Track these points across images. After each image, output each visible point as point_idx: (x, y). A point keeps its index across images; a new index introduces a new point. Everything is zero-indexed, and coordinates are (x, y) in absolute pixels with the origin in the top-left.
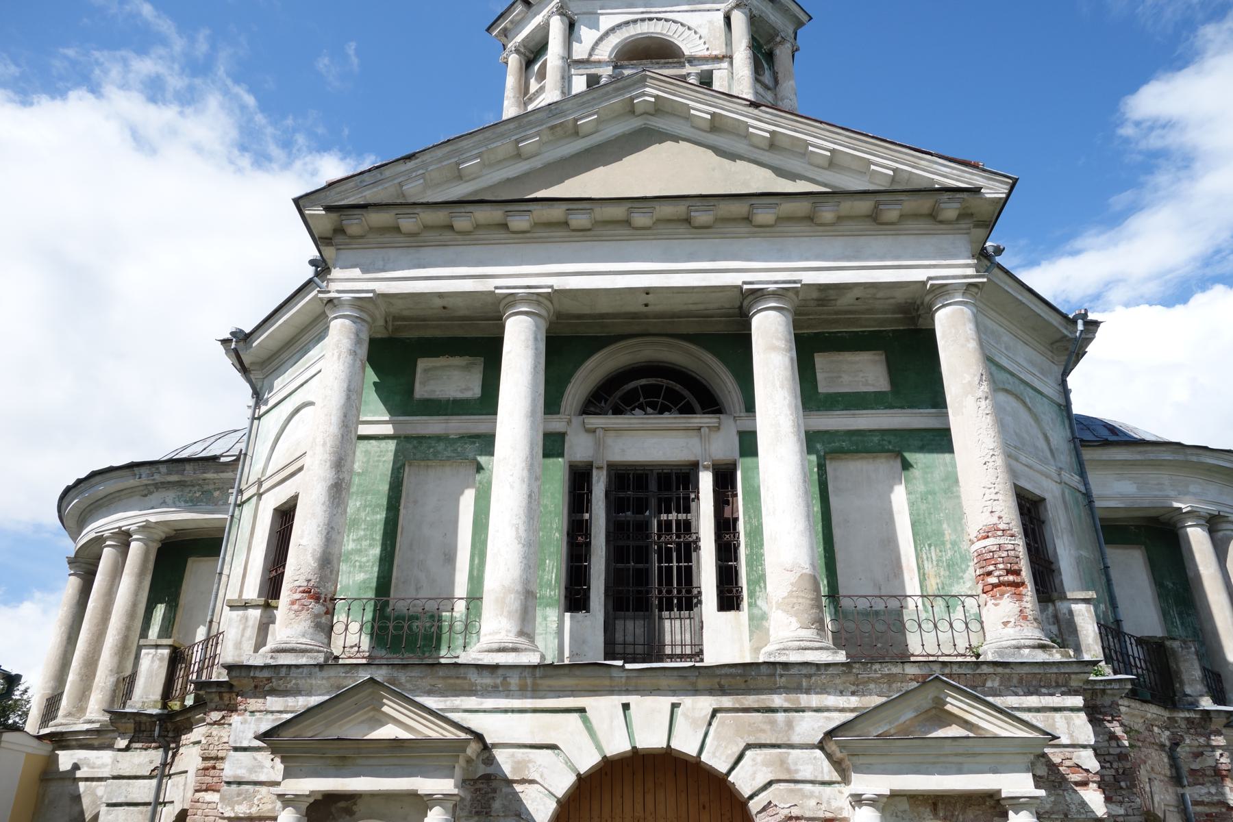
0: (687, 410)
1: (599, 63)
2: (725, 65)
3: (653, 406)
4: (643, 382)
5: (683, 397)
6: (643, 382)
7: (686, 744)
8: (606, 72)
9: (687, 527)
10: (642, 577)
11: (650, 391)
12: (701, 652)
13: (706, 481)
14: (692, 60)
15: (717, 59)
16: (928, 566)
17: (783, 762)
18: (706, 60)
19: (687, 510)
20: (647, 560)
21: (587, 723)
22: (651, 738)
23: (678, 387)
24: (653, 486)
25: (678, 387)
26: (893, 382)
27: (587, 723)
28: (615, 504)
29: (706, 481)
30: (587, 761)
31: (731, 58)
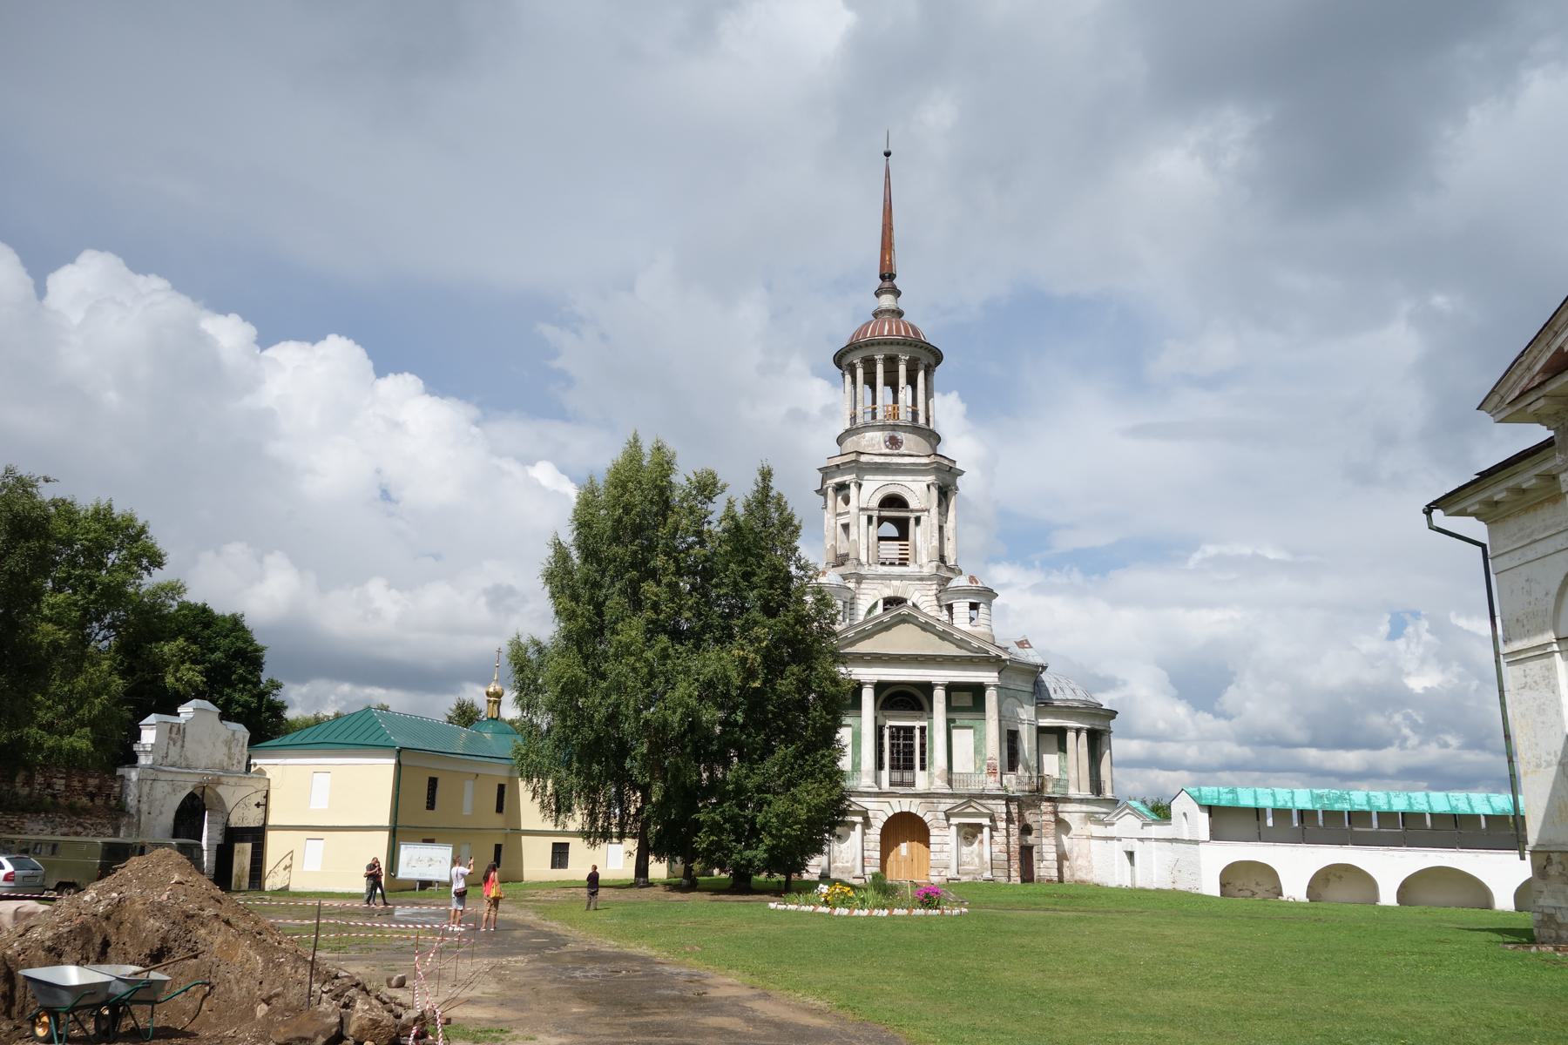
0: (913, 709)
1: (872, 510)
2: (926, 513)
4: (898, 698)
5: (910, 703)
6: (898, 698)
9: (912, 746)
10: (898, 759)
11: (902, 701)
12: (914, 782)
13: (917, 733)
14: (912, 511)
15: (923, 511)
16: (977, 762)
17: (935, 815)
18: (917, 511)
20: (904, 759)
22: (905, 809)
24: (902, 732)
26: (974, 704)
28: (892, 737)
29: (917, 733)
30: (891, 814)
31: (929, 511)
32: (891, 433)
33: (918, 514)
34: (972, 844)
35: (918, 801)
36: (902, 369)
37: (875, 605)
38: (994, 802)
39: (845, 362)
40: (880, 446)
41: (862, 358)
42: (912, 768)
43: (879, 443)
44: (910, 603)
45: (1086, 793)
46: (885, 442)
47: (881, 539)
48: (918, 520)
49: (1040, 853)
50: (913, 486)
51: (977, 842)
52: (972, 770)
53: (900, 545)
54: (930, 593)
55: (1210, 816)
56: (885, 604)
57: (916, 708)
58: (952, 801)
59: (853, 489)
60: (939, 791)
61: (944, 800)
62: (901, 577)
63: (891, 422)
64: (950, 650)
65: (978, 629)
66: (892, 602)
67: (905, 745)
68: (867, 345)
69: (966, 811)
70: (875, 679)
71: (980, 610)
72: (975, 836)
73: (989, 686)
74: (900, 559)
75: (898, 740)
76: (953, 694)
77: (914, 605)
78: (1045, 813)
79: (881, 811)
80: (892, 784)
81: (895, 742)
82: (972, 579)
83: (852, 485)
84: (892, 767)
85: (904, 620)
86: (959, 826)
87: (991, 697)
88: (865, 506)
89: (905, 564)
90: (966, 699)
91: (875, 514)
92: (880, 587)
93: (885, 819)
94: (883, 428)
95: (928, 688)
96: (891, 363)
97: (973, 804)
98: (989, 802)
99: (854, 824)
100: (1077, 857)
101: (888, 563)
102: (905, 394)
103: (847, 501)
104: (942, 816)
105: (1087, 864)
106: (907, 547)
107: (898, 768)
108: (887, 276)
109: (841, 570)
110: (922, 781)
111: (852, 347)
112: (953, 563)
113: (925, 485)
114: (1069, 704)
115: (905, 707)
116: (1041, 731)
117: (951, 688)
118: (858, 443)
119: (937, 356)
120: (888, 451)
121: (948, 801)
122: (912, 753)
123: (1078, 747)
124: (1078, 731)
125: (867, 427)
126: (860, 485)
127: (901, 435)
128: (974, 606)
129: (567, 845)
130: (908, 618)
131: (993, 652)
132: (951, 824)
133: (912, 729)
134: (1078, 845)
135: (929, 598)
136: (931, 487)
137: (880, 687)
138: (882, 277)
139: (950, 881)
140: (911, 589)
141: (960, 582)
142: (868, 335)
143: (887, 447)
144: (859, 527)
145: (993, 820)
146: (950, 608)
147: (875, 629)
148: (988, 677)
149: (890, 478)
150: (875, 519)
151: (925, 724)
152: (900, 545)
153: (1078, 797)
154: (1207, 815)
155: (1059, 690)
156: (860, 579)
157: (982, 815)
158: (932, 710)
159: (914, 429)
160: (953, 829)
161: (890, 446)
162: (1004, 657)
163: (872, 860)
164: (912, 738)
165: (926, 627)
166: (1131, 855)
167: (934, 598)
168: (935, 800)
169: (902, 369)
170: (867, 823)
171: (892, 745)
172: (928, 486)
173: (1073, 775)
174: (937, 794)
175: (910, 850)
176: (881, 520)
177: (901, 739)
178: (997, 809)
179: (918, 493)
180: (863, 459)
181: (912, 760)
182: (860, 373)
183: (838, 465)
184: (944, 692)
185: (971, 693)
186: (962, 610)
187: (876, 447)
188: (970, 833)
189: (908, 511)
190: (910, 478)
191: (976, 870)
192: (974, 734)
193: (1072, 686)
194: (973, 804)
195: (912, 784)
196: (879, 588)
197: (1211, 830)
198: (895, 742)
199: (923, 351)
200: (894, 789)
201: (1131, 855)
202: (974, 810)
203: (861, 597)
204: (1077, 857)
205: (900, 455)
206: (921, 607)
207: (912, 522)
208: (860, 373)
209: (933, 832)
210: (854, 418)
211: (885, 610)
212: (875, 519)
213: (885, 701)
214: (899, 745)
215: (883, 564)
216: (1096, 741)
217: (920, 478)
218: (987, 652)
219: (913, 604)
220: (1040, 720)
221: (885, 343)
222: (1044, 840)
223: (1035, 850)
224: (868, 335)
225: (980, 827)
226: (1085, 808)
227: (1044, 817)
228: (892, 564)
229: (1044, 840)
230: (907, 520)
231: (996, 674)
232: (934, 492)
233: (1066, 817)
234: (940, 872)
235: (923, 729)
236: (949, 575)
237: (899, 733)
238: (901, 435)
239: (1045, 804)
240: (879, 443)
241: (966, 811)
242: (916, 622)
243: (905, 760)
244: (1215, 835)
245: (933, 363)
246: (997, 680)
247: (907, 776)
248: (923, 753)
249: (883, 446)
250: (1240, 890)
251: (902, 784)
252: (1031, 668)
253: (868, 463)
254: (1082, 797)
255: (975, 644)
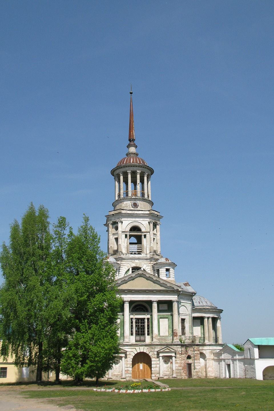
0: (144, 311)
1: (127, 232)
2: (148, 233)
3: (140, 310)
4: (138, 307)
6: (138, 307)
7: (145, 351)
8: (128, 234)
9: (144, 326)
11: (140, 308)
12: (145, 340)
13: (146, 321)
14: (143, 232)
19: (144, 324)
21: (136, 349)
22: (142, 351)
23: (143, 308)
24: (140, 320)
25: (143, 308)
26: (168, 309)
27: (136, 349)
28: (136, 323)
29: (146, 321)
30: (136, 353)
31: (149, 232)
32: (134, 202)
33: (145, 234)
34: (168, 363)
35: (146, 348)
36: (138, 176)
37: (129, 270)
38: (176, 347)
39: (115, 173)
40: (129, 207)
41: (122, 172)
42: (144, 334)
43: (129, 205)
44: (142, 269)
45: (212, 342)
46: (132, 205)
47: (130, 243)
48: (145, 236)
49: (194, 366)
50: (143, 223)
51: (170, 363)
52: (167, 334)
53: (138, 246)
54: (150, 265)
55: (259, 349)
56: (132, 270)
57: (145, 310)
58: (160, 347)
59: (120, 225)
60: (155, 343)
61: (157, 347)
62: (139, 259)
63: (134, 197)
64: (158, 287)
65: (169, 279)
66: (136, 269)
67: (141, 326)
68: (124, 167)
69: (165, 351)
70: (129, 299)
71: (170, 272)
72: (169, 361)
73: (174, 301)
74: (138, 252)
75: (139, 323)
76: (160, 305)
77: (144, 270)
78: (196, 351)
79: (132, 352)
80: (136, 341)
81: (137, 324)
82: (167, 259)
83: (119, 222)
84: (137, 334)
85: (140, 276)
86: (163, 357)
87: (175, 305)
88: (124, 231)
89: (140, 254)
90: (165, 307)
91: (128, 234)
92: (130, 263)
93: (134, 355)
94: (131, 199)
95: (150, 303)
96: (134, 174)
97: (169, 348)
98: (175, 347)
99: (121, 357)
100: (208, 367)
101: (133, 253)
102: (139, 187)
103: (117, 228)
104: (156, 353)
105: (212, 370)
106: (141, 247)
107: (139, 335)
108: (131, 140)
109: (115, 256)
110: (148, 339)
111: (118, 167)
112: (159, 253)
113: (147, 222)
114: (204, 307)
115: (141, 310)
116: (194, 318)
117: (159, 302)
118: (121, 206)
119: (152, 171)
120: (133, 209)
121: (159, 347)
122: (144, 328)
123: (208, 324)
124: (208, 318)
125: (124, 199)
126: (122, 222)
127: (138, 202)
128: (168, 270)
129: (6, 368)
130: (142, 275)
131: (176, 288)
132: (160, 356)
133: (144, 319)
134: (208, 363)
135: (150, 267)
136: (150, 223)
137: (131, 303)
138: (130, 140)
139: (160, 379)
140: (143, 263)
141: (163, 260)
142: (125, 163)
143: (133, 207)
144: (121, 239)
145: (176, 354)
146: (158, 271)
147: (129, 280)
148: (173, 298)
149: (134, 219)
150: (128, 236)
151: (149, 316)
152: (138, 246)
153: (208, 344)
154: (258, 349)
155: (200, 302)
156: (122, 259)
157: (171, 352)
158: (152, 311)
159: (144, 200)
160: (161, 358)
161: (134, 207)
162: (180, 290)
163: (129, 371)
164: (144, 323)
165: (148, 279)
166: (229, 366)
167: (151, 267)
168: (153, 347)
169: (138, 176)
170: (126, 357)
171: (136, 326)
172: (149, 223)
173: (207, 335)
174: (154, 344)
175: (144, 367)
176: (131, 236)
177: (140, 323)
178: (178, 349)
179: (145, 225)
180: (123, 212)
181: (144, 331)
182: (122, 178)
183: (113, 214)
184: (156, 304)
185: (167, 304)
186: (163, 271)
187: (128, 207)
188: (167, 359)
189: (141, 233)
190: (142, 219)
191: (169, 374)
192: (168, 321)
193: (206, 300)
194: (169, 348)
195: (144, 341)
196: (130, 263)
197: (259, 355)
198: (137, 324)
199: (146, 169)
200: (137, 343)
201: (229, 366)
202: (169, 350)
203: (123, 267)
204: (208, 367)
205: (137, 210)
206: (147, 271)
207: (143, 237)
208: (122, 178)
209: (153, 359)
210: (119, 195)
211: (132, 272)
212: (128, 236)
213: (133, 308)
214: (139, 325)
215: (131, 254)
216: (214, 320)
217: (146, 219)
218: (173, 288)
219: (144, 269)
220: (193, 314)
221: (131, 166)
222: (195, 361)
223: (192, 365)
224: (125, 163)
225: (171, 357)
226: (211, 348)
227: (196, 352)
228: (135, 254)
229: (195, 361)
230: (141, 236)
231: (177, 296)
232: (152, 225)
233: (204, 352)
234: (156, 375)
235: (148, 319)
236: (157, 257)
237: (139, 321)
238: (138, 202)
239: (196, 347)
240: (129, 205)
241: (165, 351)
242: (145, 277)
243: (141, 331)
244: (261, 357)
245: (150, 174)
246: (177, 299)
247: (142, 338)
248: (148, 328)
249: (131, 207)
250: (270, 377)
251: (140, 341)
252: (190, 294)
253: (125, 214)
254: (210, 344)
255: (168, 285)
